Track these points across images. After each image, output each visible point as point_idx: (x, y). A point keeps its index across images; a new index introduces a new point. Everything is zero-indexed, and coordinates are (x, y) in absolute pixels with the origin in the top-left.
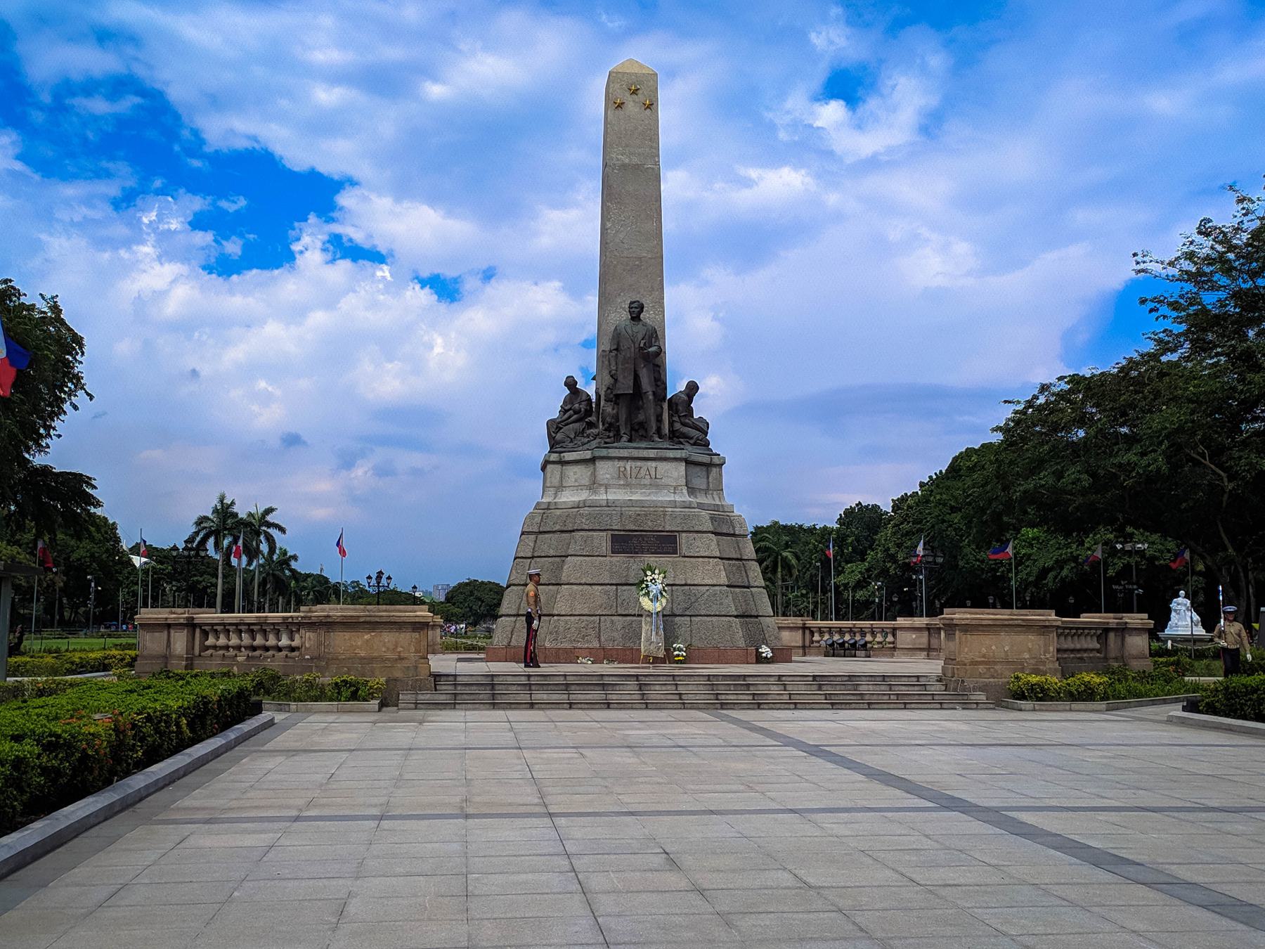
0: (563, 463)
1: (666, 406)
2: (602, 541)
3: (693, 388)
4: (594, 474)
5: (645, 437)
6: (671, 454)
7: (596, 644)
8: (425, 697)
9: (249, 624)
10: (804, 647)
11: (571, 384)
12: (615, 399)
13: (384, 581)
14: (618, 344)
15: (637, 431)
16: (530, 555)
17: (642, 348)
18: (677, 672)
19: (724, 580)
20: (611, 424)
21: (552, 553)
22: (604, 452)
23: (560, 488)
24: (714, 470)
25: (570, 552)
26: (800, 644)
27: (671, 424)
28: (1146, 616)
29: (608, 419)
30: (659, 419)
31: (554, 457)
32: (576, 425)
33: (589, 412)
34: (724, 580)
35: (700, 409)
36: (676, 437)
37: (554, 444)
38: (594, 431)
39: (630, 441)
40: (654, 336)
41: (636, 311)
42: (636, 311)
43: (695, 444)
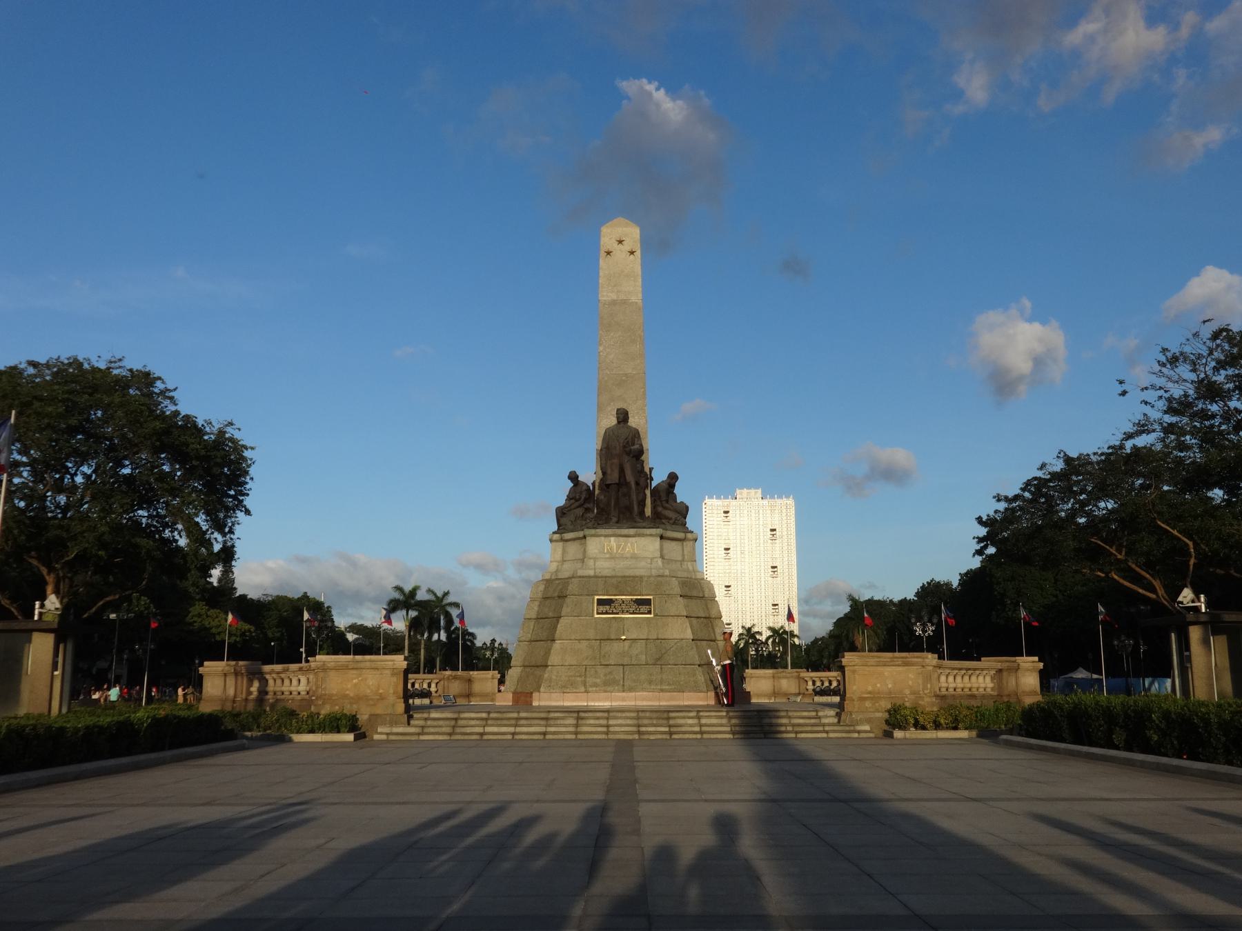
0: (562, 540)
1: (648, 492)
3: (673, 478)
4: (585, 551)
6: (648, 531)
11: (573, 477)
12: (604, 485)
21: (551, 614)
22: (593, 531)
23: (564, 561)
24: (688, 544)
27: (654, 508)
28: (1036, 659)
30: (642, 504)
31: (556, 536)
32: (580, 511)
33: (586, 500)
34: (689, 635)
35: (682, 493)
36: (658, 519)
37: (561, 528)
38: (590, 515)
40: (636, 435)
41: (623, 416)
42: (623, 416)
43: (674, 523)
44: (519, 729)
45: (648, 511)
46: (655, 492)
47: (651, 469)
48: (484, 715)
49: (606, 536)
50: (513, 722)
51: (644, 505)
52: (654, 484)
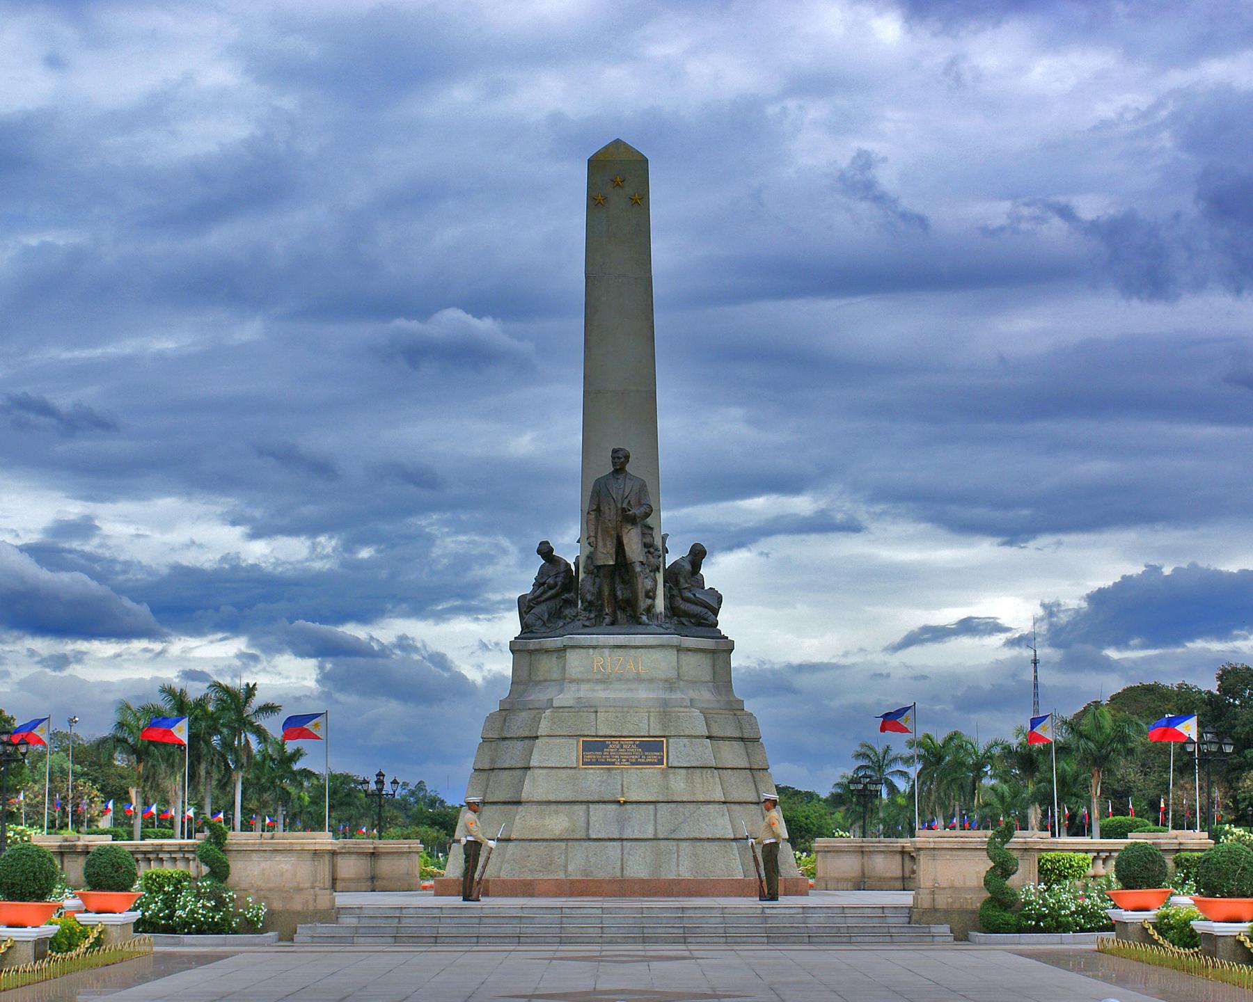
2: (571, 753)
3: (698, 555)
5: (635, 620)
7: (561, 876)
8: (322, 929)
9: (145, 853)
10: (903, 878)
13: (388, 788)
14: (599, 506)
15: (623, 610)
16: (487, 766)
17: (623, 510)
18: (606, 905)
19: (719, 796)
20: (590, 603)
25: (532, 764)
26: (899, 873)
27: (670, 598)
29: (589, 597)
30: (651, 595)
32: (551, 604)
39: (613, 623)
41: (620, 461)
42: (620, 461)
43: (699, 624)
44: (482, 930)
45: (660, 604)
46: (672, 576)
47: (664, 538)
48: (436, 913)
49: (594, 647)
50: (477, 921)
51: (654, 598)
52: (670, 560)
